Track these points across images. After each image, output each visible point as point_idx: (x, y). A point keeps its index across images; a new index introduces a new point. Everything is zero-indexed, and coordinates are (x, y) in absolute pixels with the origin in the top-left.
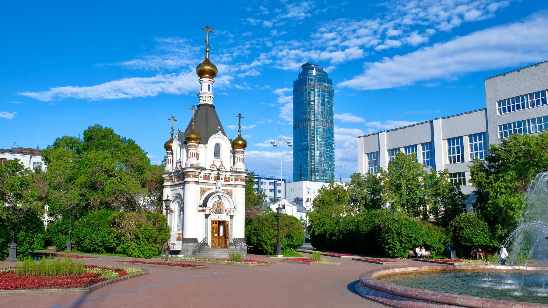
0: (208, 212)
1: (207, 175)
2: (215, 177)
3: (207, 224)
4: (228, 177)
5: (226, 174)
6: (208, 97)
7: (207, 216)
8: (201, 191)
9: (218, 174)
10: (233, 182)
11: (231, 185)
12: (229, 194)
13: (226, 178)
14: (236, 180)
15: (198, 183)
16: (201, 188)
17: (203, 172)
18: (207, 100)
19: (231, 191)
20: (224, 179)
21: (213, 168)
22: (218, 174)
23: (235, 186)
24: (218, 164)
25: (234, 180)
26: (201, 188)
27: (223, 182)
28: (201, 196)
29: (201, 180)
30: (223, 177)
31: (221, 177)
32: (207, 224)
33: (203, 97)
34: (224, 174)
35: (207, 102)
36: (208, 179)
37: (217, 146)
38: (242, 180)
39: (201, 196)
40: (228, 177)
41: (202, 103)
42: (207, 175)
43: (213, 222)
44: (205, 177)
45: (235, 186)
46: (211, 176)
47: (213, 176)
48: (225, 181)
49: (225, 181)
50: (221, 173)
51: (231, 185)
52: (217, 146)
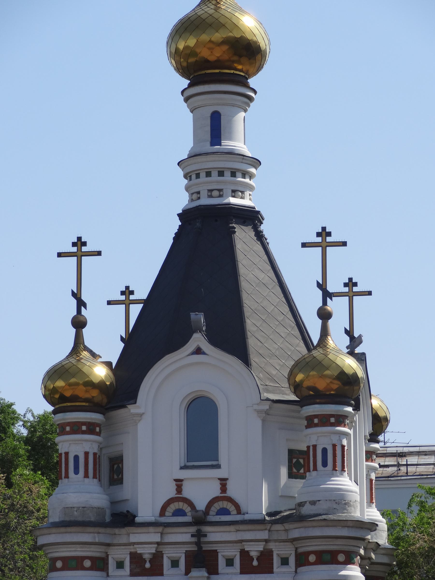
1: (147, 551)
2: (188, 554)
4: (254, 550)
13: (244, 554)
18: (204, 194)
20: (237, 561)
21: (179, 512)
24: (201, 490)
25: (292, 561)
30: (233, 552)
31: (225, 552)
34: (233, 537)
35: (205, 201)
42: (147, 551)
44: (136, 558)
46: (169, 554)
50: (215, 535)
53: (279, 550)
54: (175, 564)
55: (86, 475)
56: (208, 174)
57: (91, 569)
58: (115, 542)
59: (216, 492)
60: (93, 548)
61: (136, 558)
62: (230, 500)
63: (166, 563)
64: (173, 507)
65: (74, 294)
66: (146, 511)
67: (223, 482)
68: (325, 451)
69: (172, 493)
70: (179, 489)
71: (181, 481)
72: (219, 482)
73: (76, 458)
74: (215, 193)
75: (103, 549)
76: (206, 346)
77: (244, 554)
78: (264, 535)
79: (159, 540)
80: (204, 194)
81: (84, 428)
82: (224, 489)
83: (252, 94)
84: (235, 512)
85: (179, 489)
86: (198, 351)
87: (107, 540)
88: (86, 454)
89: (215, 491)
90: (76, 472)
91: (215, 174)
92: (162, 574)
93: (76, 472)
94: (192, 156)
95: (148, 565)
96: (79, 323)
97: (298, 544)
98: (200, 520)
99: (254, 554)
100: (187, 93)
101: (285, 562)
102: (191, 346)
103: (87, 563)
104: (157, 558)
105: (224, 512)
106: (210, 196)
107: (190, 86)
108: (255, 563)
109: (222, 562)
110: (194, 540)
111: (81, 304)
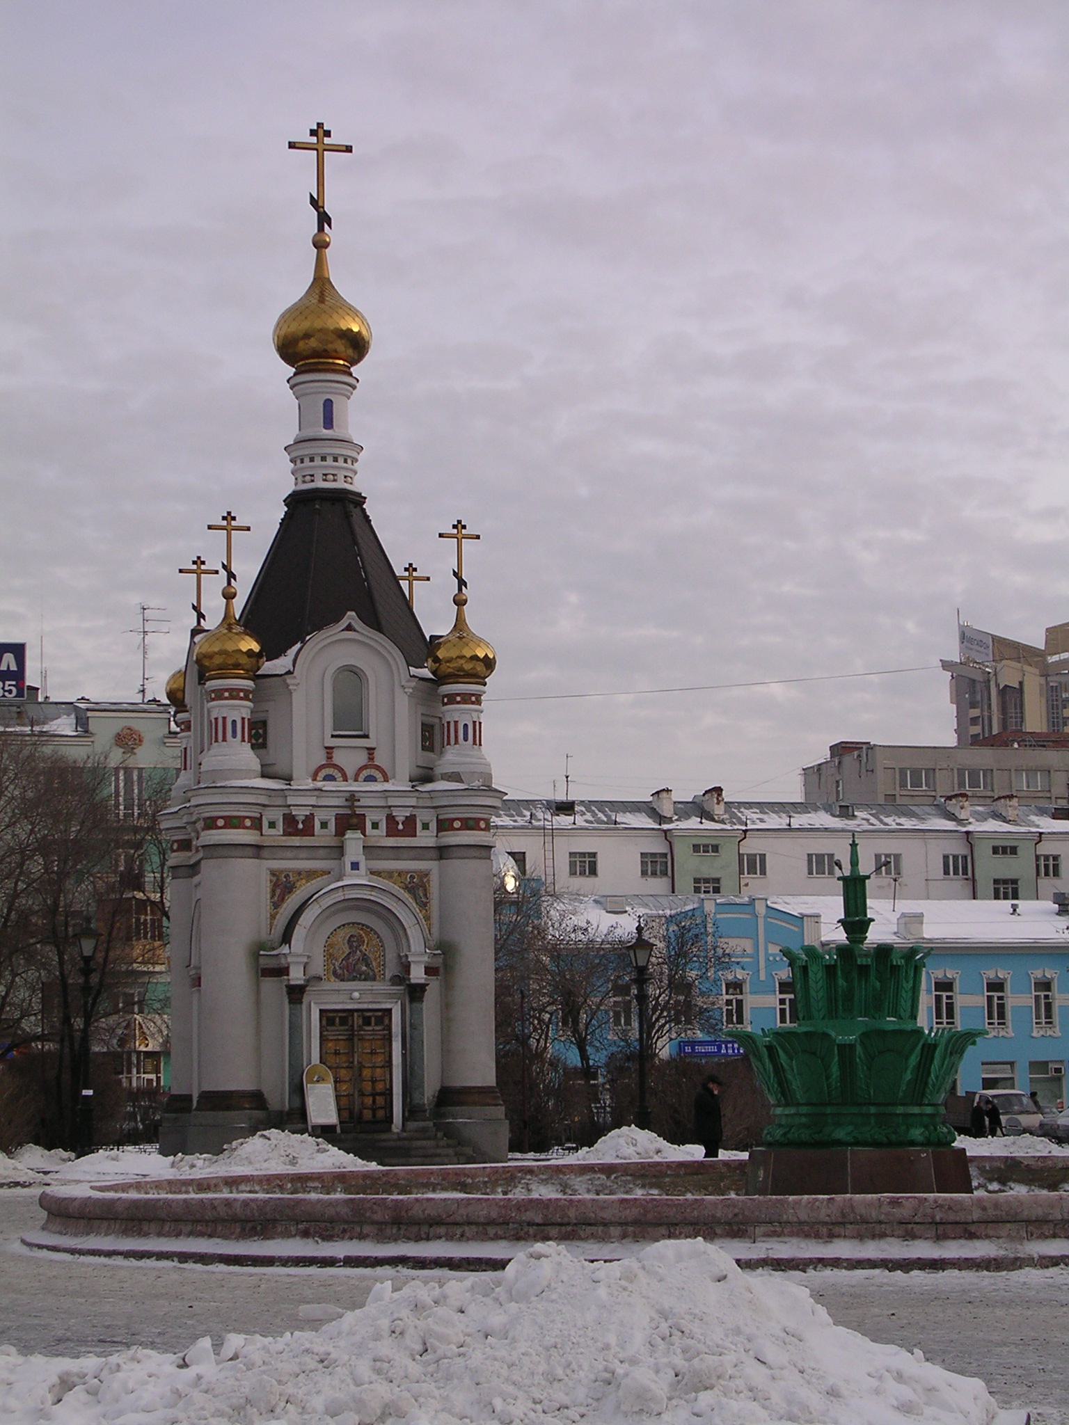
1: (301, 813)
2: (338, 817)
4: (401, 815)
5: (391, 802)
7: (296, 994)
8: (275, 885)
10: (425, 838)
11: (419, 852)
12: (410, 889)
13: (391, 819)
14: (444, 826)
15: (257, 850)
16: (273, 873)
18: (319, 477)
20: (383, 825)
23: (442, 852)
25: (433, 826)
26: (273, 873)
27: (379, 837)
28: (276, 905)
30: (381, 817)
32: (295, 1029)
36: (308, 831)
39: (276, 905)
40: (401, 815)
42: (301, 813)
43: (328, 1017)
44: (290, 820)
45: (442, 852)
46: (319, 816)
47: (330, 816)
48: (392, 831)
49: (392, 831)
51: (419, 852)
53: (422, 816)
54: (324, 825)
56: (312, 460)
60: (254, 808)
61: (290, 820)
64: (365, 773)
67: (371, 750)
70: (330, 758)
71: (332, 748)
72: (366, 752)
73: (234, 722)
75: (259, 809)
76: (358, 624)
77: (391, 819)
80: (319, 477)
81: (242, 694)
82: (371, 759)
85: (330, 758)
86: (349, 628)
89: (362, 758)
90: (234, 735)
91: (307, 460)
94: (298, 442)
95: (301, 826)
96: (460, 602)
97: (440, 811)
99: (400, 819)
100: (292, 382)
101: (426, 826)
102: (344, 623)
104: (309, 819)
106: (304, 482)
107: (295, 374)
108: (401, 827)
111: (462, 583)
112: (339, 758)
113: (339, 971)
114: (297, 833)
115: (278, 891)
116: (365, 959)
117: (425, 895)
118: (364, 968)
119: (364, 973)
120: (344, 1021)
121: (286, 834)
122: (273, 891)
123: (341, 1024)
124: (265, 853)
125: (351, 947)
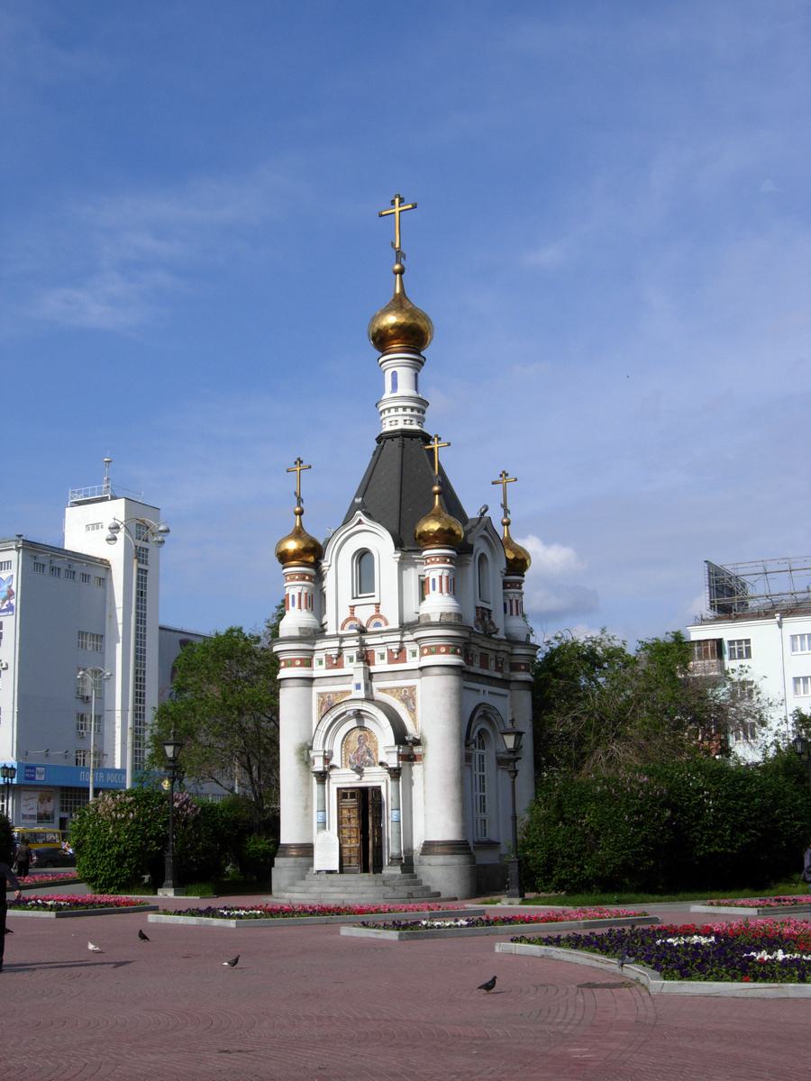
0: (319, 765)
3: (323, 800)
4: (395, 647)
6: (396, 408)
7: (323, 777)
9: (363, 645)
10: (413, 662)
13: (390, 651)
17: (320, 645)
19: (412, 689)
20: (386, 657)
21: (351, 627)
22: (363, 645)
26: (321, 695)
29: (318, 670)
30: (383, 650)
31: (378, 651)
32: (323, 800)
33: (389, 409)
36: (339, 665)
37: (363, 555)
38: (434, 651)
41: (387, 428)
42: (334, 652)
43: (343, 794)
44: (329, 658)
48: (391, 661)
50: (369, 640)
52: (363, 555)
55: (300, 608)
57: (300, 666)
58: (315, 648)
59: (373, 613)
61: (329, 658)
62: (381, 617)
63: (346, 659)
65: (295, 494)
66: (331, 630)
67: (377, 605)
68: (434, 580)
69: (348, 615)
74: (394, 423)
76: (364, 518)
77: (390, 651)
78: (398, 638)
79: (338, 645)
83: (423, 360)
84: (383, 625)
86: (360, 522)
87: (310, 647)
88: (300, 594)
89: (372, 610)
92: (343, 667)
93: (293, 605)
97: (422, 641)
98: (362, 631)
100: (381, 360)
101: (414, 654)
103: (298, 663)
105: (378, 624)
108: (396, 656)
109: (377, 657)
110: (358, 644)
112: (359, 613)
113: (353, 761)
114: (397, 661)
115: (324, 708)
116: (369, 752)
117: (414, 704)
118: (368, 758)
119: (368, 761)
120: (353, 796)
121: (327, 668)
122: (321, 708)
123: (351, 798)
124: (316, 682)
125: (360, 743)
